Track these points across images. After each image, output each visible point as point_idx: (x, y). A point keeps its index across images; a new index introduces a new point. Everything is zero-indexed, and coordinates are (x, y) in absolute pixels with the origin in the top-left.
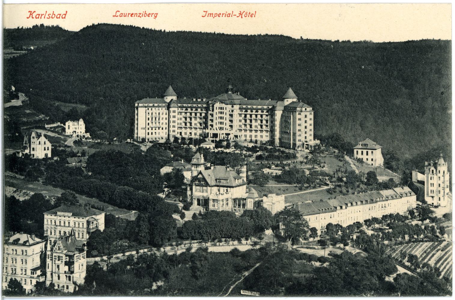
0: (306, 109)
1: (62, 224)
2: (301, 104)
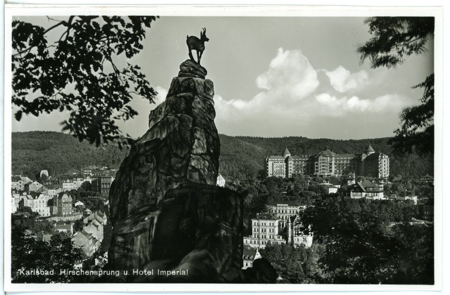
0: (385, 157)
2: (381, 154)
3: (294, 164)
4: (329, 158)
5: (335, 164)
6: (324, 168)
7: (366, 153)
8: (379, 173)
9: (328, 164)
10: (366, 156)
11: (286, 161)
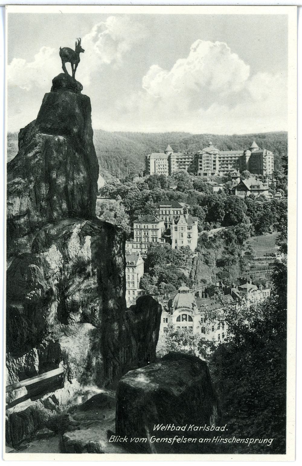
1: (164, 213)
3: (177, 162)
4: (213, 156)
5: (220, 161)
6: (208, 165)
7: (251, 149)
8: (264, 171)
9: (212, 161)
10: (251, 153)
11: (169, 159)
